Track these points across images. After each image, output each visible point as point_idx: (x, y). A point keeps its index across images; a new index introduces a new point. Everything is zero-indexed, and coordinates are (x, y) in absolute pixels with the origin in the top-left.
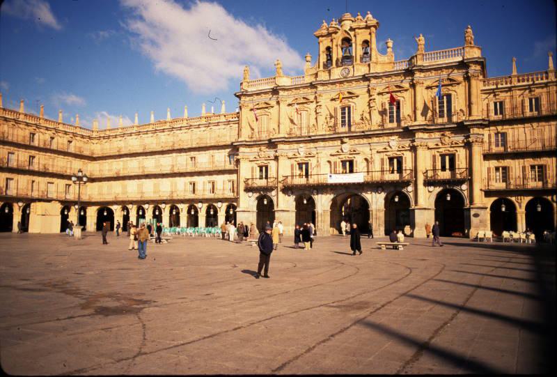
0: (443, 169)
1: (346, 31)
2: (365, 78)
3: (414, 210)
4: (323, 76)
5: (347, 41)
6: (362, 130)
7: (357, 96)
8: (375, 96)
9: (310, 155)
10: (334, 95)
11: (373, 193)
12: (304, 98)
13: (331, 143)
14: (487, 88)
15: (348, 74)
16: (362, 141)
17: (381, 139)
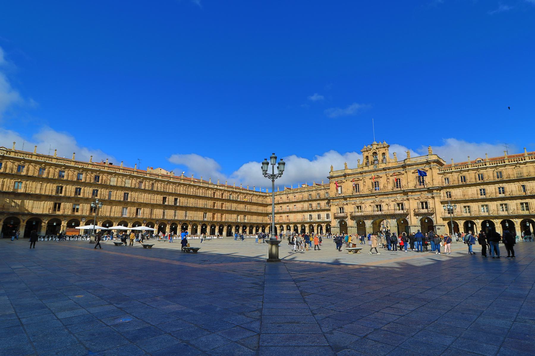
0: (423, 208)
1: (374, 149)
2: (384, 169)
3: (410, 226)
4: (366, 169)
5: (375, 153)
6: (384, 192)
7: (381, 177)
8: (390, 177)
9: (362, 203)
10: (370, 177)
11: (391, 220)
12: (358, 178)
13: (371, 198)
14: (441, 172)
15: (377, 167)
16: (385, 196)
17: (393, 196)
